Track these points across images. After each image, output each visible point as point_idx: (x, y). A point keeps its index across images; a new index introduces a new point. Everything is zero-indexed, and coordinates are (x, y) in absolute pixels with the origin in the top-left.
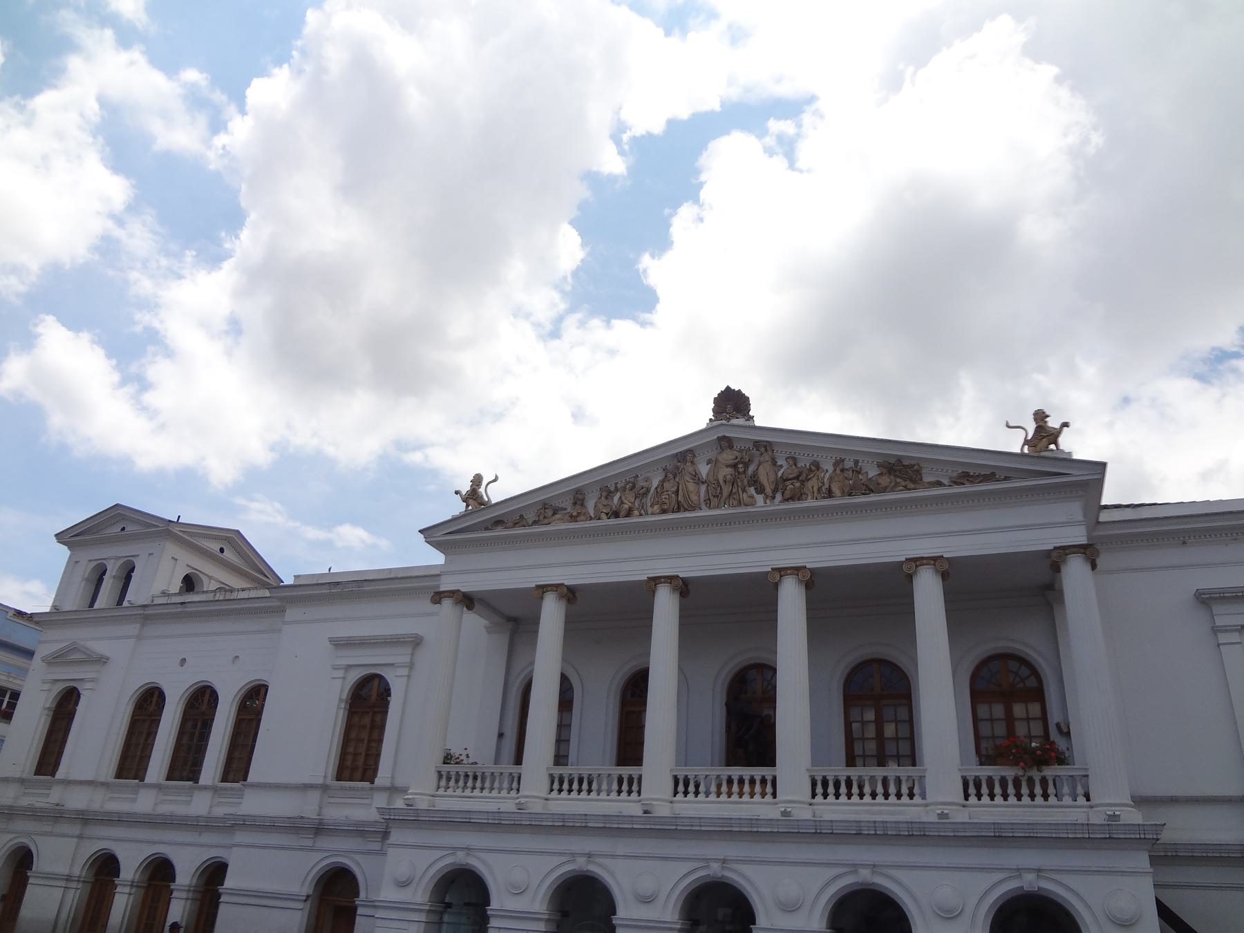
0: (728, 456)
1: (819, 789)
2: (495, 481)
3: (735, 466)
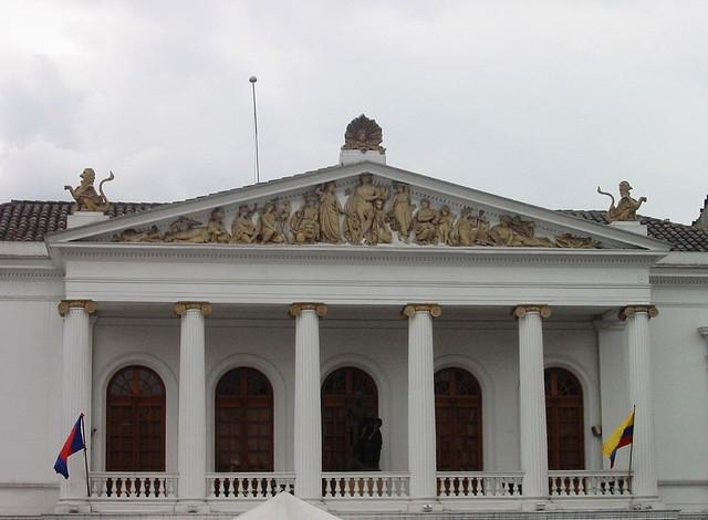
0: (366, 191)
1: (443, 488)
2: (110, 179)
3: (373, 202)
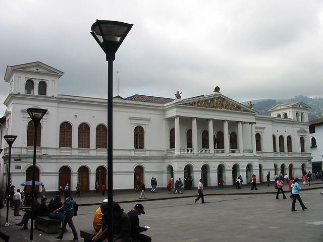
0: (219, 99)
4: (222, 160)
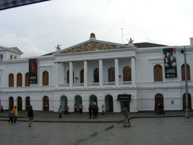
0: (92, 43)
4: (29, 94)
